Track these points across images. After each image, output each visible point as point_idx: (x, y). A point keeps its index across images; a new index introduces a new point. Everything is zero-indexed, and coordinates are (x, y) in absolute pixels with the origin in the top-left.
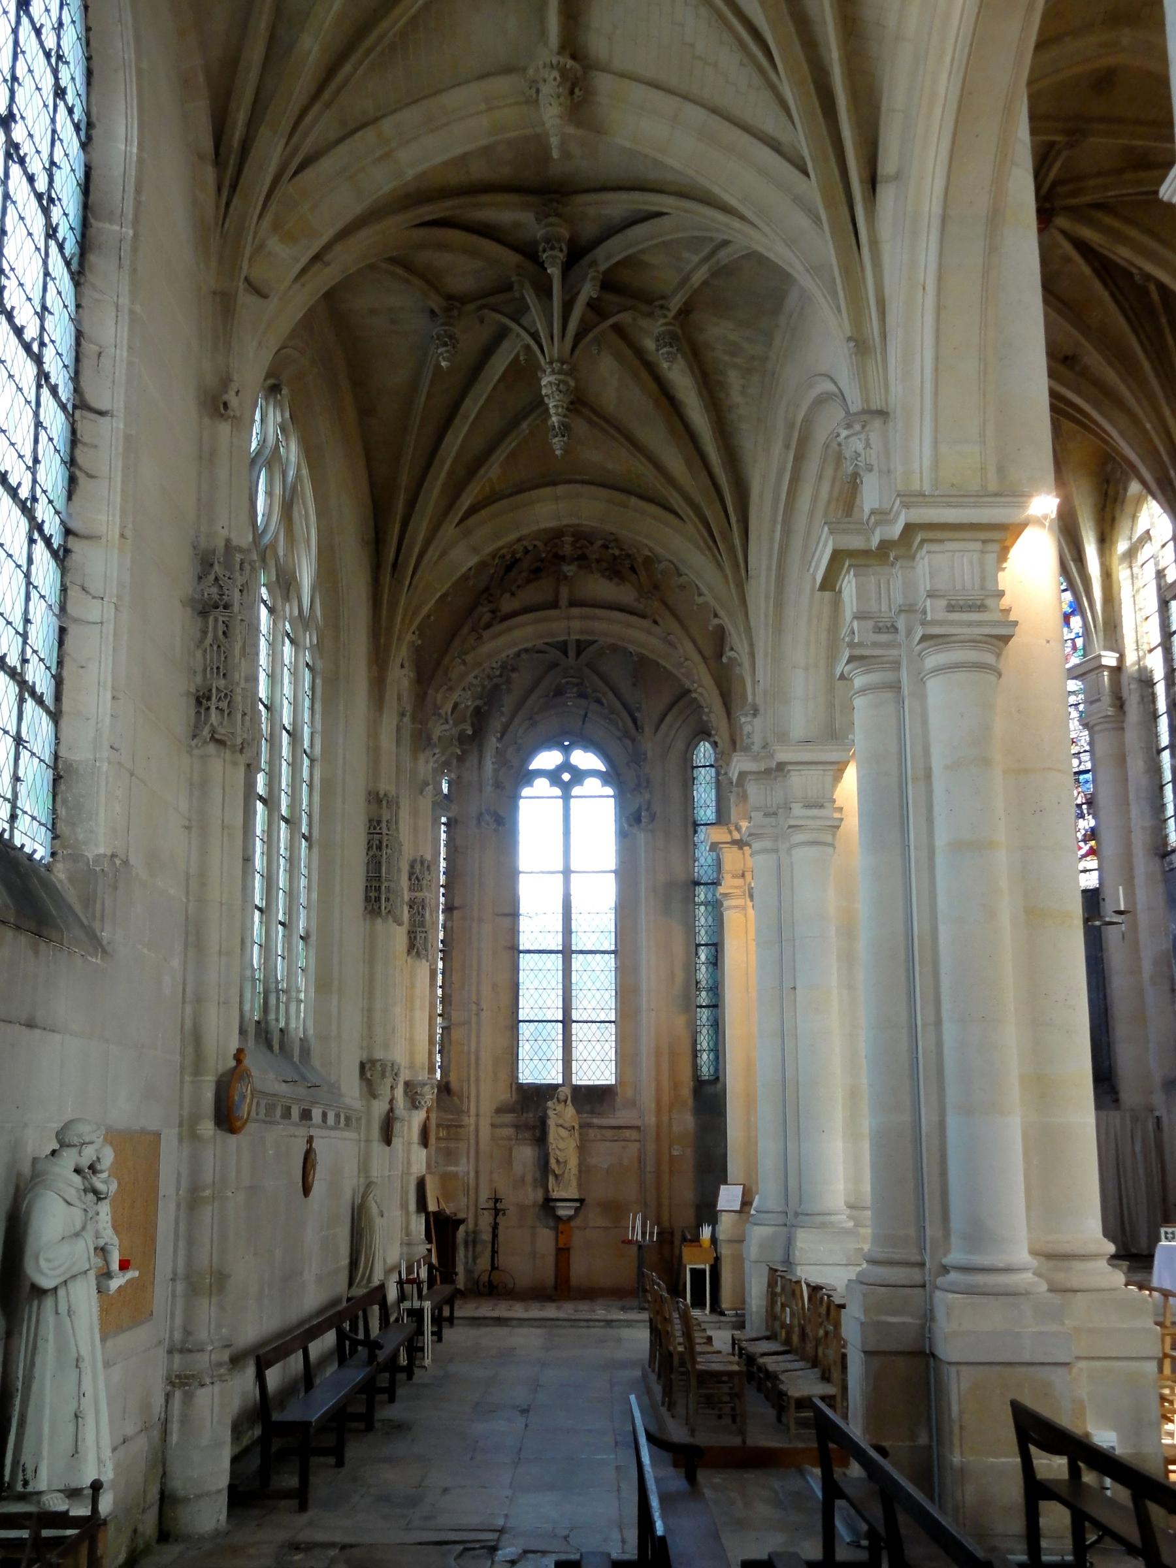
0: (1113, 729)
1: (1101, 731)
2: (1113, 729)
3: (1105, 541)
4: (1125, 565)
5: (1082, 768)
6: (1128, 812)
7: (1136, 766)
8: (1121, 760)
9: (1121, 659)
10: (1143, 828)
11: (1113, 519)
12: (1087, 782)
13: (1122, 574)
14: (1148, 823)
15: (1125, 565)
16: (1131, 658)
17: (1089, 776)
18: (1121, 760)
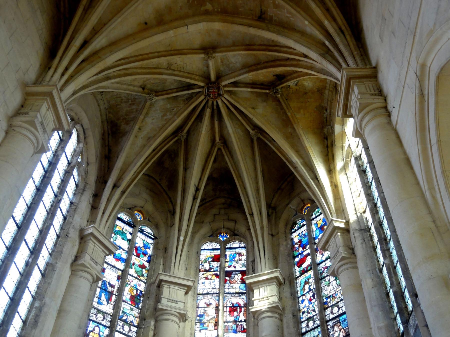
0: (350, 268)
1: (342, 271)
2: (350, 268)
3: (331, 171)
4: (343, 173)
5: (341, 312)
6: (369, 323)
7: (368, 283)
8: (358, 287)
9: (347, 223)
10: (380, 328)
11: (333, 156)
12: (345, 320)
13: (341, 178)
14: (382, 324)
15: (343, 173)
16: (353, 218)
17: (344, 316)
18: (358, 287)
